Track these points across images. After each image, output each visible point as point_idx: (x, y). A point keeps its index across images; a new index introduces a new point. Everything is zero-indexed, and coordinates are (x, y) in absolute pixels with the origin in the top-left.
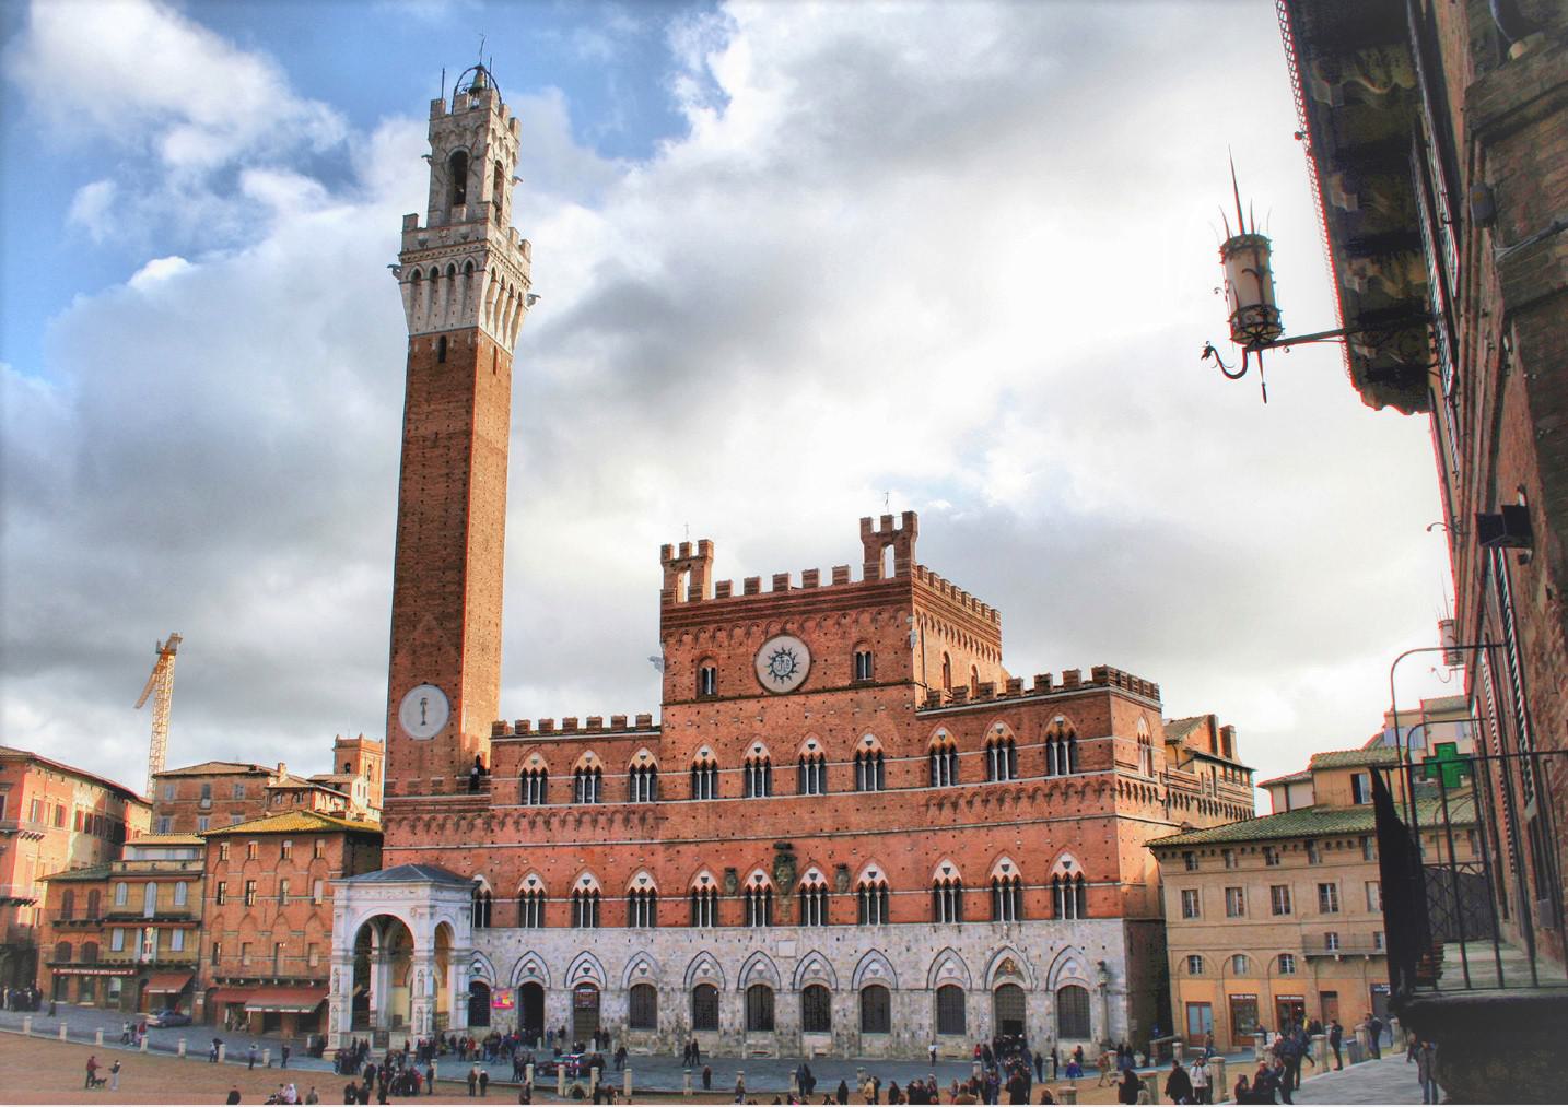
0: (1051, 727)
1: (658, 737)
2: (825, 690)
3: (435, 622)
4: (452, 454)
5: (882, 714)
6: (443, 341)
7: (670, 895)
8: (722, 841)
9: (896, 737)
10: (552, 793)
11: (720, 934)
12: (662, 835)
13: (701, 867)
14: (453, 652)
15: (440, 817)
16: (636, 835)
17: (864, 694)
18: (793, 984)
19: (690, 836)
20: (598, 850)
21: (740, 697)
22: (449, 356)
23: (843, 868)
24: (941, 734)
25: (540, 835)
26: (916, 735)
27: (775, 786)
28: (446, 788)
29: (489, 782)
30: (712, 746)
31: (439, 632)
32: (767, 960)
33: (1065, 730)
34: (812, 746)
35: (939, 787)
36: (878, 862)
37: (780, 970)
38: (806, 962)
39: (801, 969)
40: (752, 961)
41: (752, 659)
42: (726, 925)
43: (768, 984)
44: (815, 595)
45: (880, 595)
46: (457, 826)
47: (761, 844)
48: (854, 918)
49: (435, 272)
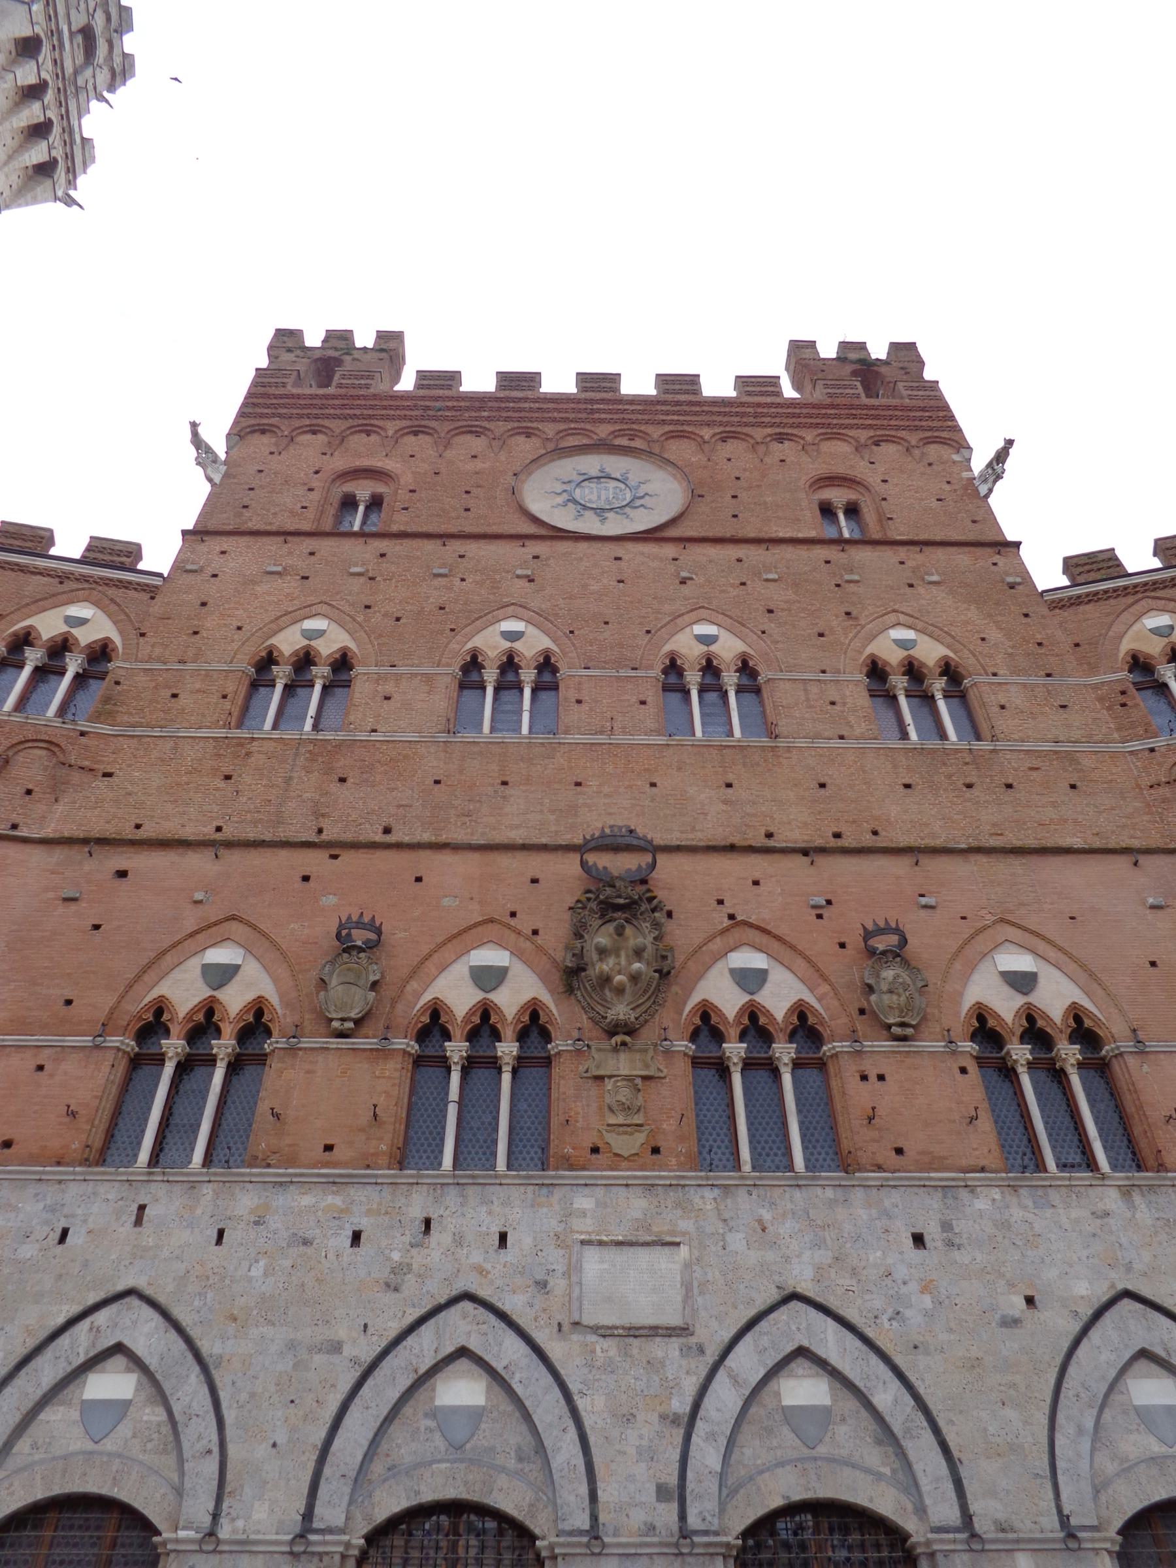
1: (152, 592)
7: (21, 1026)
8: (335, 848)
9: (994, 635)
11: (246, 1201)
13: (210, 930)
18: (680, 1495)
23: (885, 947)
32: (508, 1352)
36: (1035, 939)
37: (592, 1407)
38: (749, 1362)
39: (725, 1399)
40: (425, 1347)
41: (510, 480)
42: (291, 1161)
43: (509, 1499)
44: (698, 404)
47: (505, 861)
48: (983, 1141)
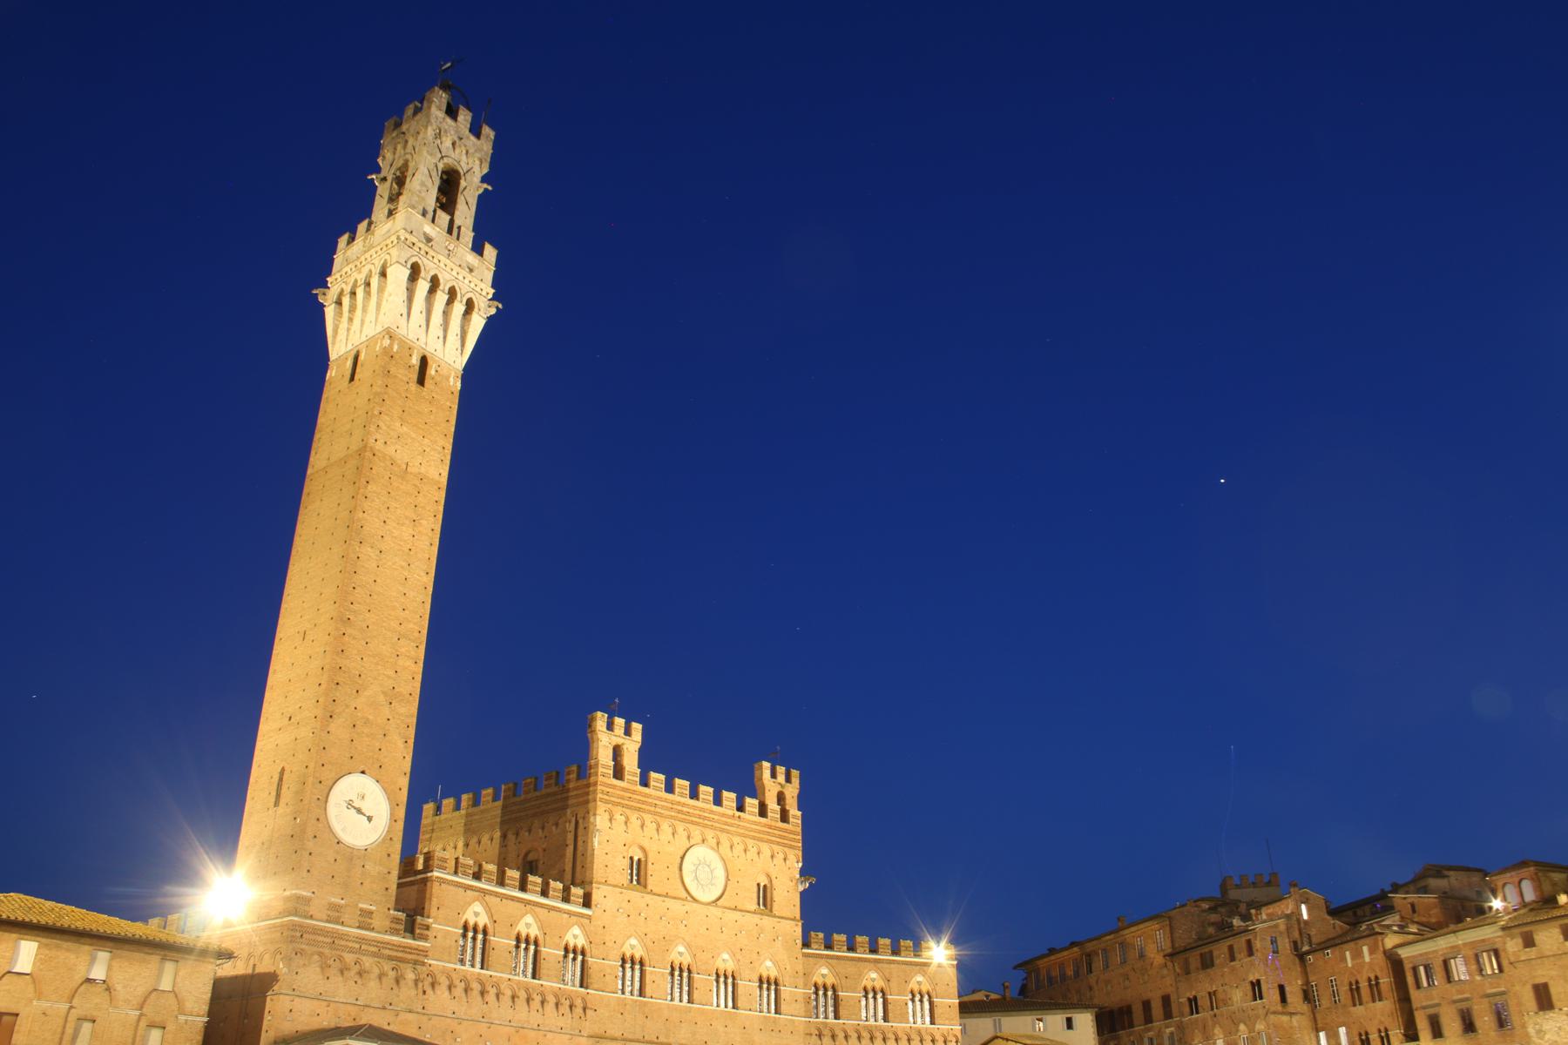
0: (913, 985)
1: (589, 917)
2: (735, 909)
3: (382, 698)
4: (420, 498)
5: (779, 943)
6: (424, 361)
10: (493, 957)
12: (589, 1026)
14: (400, 744)
15: (368, 962)
16: (566, 1021)
17: (767, 922)
19: (618, 1034)
20: (532, 1034)
21: (667, 895)
22: (428, 381)
24: (823, 973)
25: (476, 1006)
26: (800, 968)
27: (696, 995)
28: (376, 923)
29: (428, 928)
30: (641, 941)
31: (386, 711)
33: (924, 990)
34: (726, 962)
35: (821, 1019)
45: (780, 837)
46: (380, 977)
49: (435, 283)
